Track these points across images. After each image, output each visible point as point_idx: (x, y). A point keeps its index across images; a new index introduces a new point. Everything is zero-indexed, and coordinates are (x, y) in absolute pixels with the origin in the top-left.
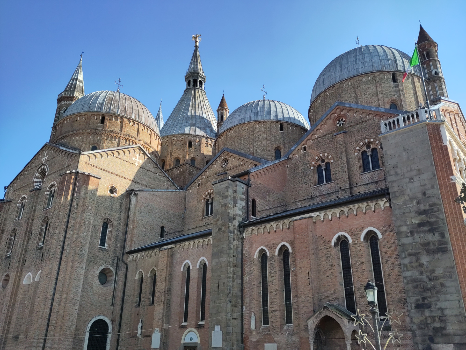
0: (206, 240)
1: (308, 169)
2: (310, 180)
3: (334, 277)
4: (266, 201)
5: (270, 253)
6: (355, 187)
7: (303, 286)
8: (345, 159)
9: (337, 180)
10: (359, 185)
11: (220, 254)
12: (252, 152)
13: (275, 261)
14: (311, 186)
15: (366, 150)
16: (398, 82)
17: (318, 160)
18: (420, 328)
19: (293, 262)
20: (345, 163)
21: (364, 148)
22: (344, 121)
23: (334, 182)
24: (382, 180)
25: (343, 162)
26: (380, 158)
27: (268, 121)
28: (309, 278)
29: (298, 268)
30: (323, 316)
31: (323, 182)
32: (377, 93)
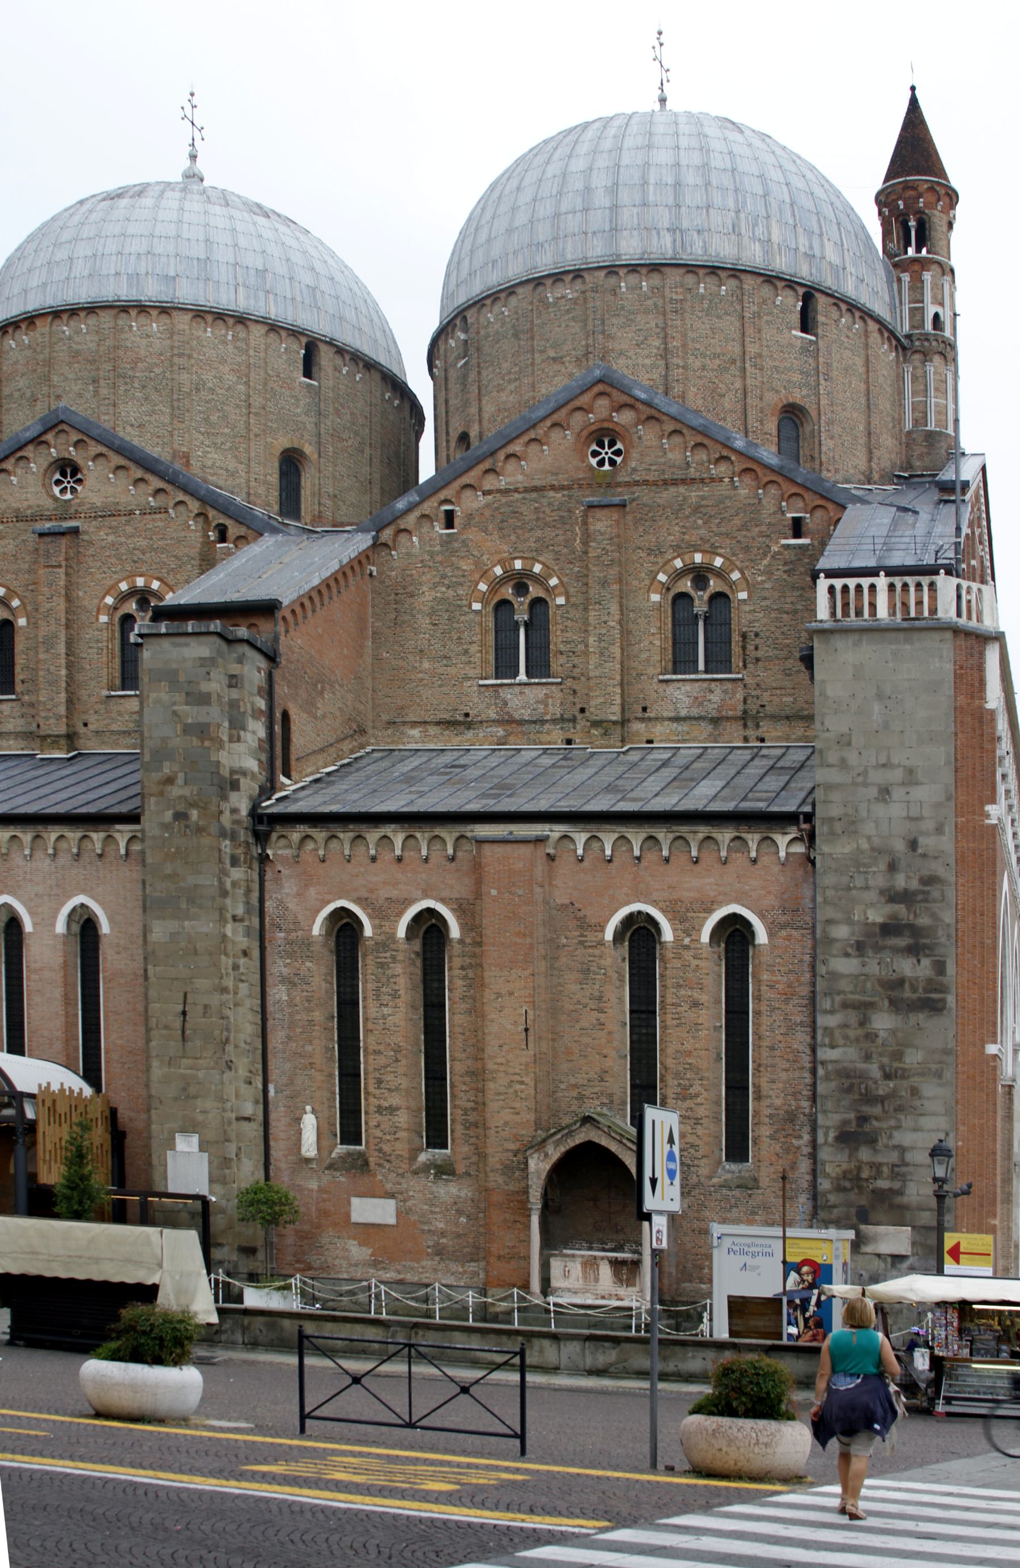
0: (94, 836)
1: (460, 606)
2: (466, 652)
3: (603, 1034)
4: (316, 717)
5: (374, 927)
6: (636, 718)
7: (505, 1048)
8: (614, 608)
9: (574, 678)
10: (652, 715)
11: (184, 906)
12: (185, 449)
13: (393, 957)
14: (468, 678)
15: (692, 593)
16: (816, 335)
17: (502, 581)
18: (839, 1189)
19: (462, 968)
20: (613, 624)
21: (686, 585)
22: (618, 453)
23: (560, 684)
24: (735, 718)
25: (606, 618)
26: (736, 638)
27: (257, 322)
28: (526, 1030)
29: (489, 995)
30: (578, 1141)
31: (516, 674)
32: (744, 361)
